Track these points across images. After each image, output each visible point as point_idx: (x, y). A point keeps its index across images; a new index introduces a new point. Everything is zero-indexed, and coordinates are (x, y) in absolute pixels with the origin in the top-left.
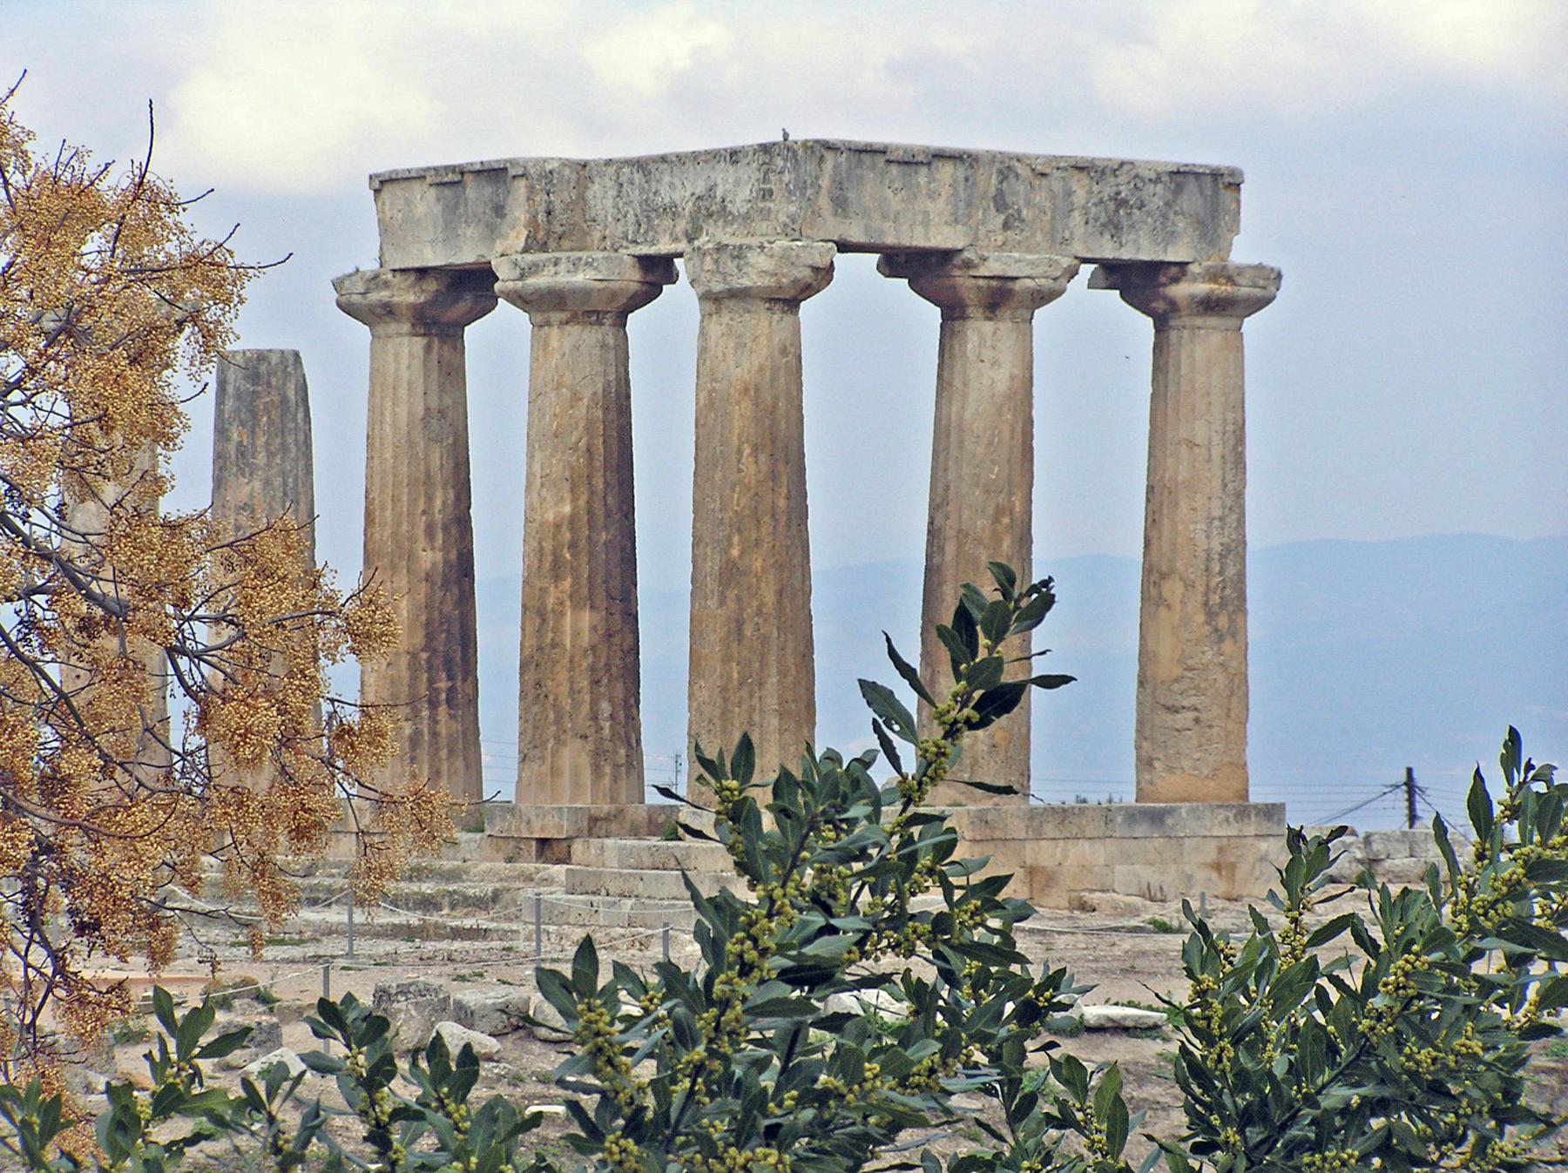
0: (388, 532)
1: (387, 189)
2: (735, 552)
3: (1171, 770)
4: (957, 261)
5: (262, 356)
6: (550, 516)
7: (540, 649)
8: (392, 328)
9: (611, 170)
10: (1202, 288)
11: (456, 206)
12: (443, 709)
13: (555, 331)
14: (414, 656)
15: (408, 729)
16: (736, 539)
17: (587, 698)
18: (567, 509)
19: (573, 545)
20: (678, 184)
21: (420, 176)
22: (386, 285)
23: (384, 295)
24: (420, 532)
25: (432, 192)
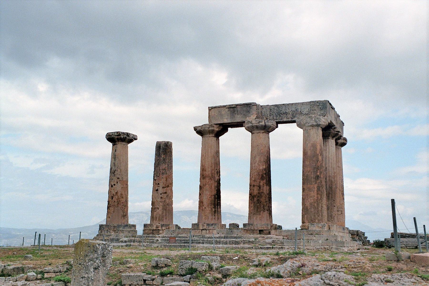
0: (210, 173)
1: (213, 109)
2: (318, 174)
3: (338, 221)
4: (333, 128)
5: (168, 142)
6: (261, 168)
7: (259, 193)
8: (211, 135)
9: (268, 107)
10: (343, 141)
11: (234, 112)
12: (219, 206)
13: (261, 134)
14: (215, 196)
15: (214, 210)
16: (319, 171)
17: (268, 203)
18: (264, 167)
19: (265, 174)
20: (287, 109)
21: (224, 106)
22: (213, 127)
23: (213, 128)
24: (216, 173)
25: (227, 109)
